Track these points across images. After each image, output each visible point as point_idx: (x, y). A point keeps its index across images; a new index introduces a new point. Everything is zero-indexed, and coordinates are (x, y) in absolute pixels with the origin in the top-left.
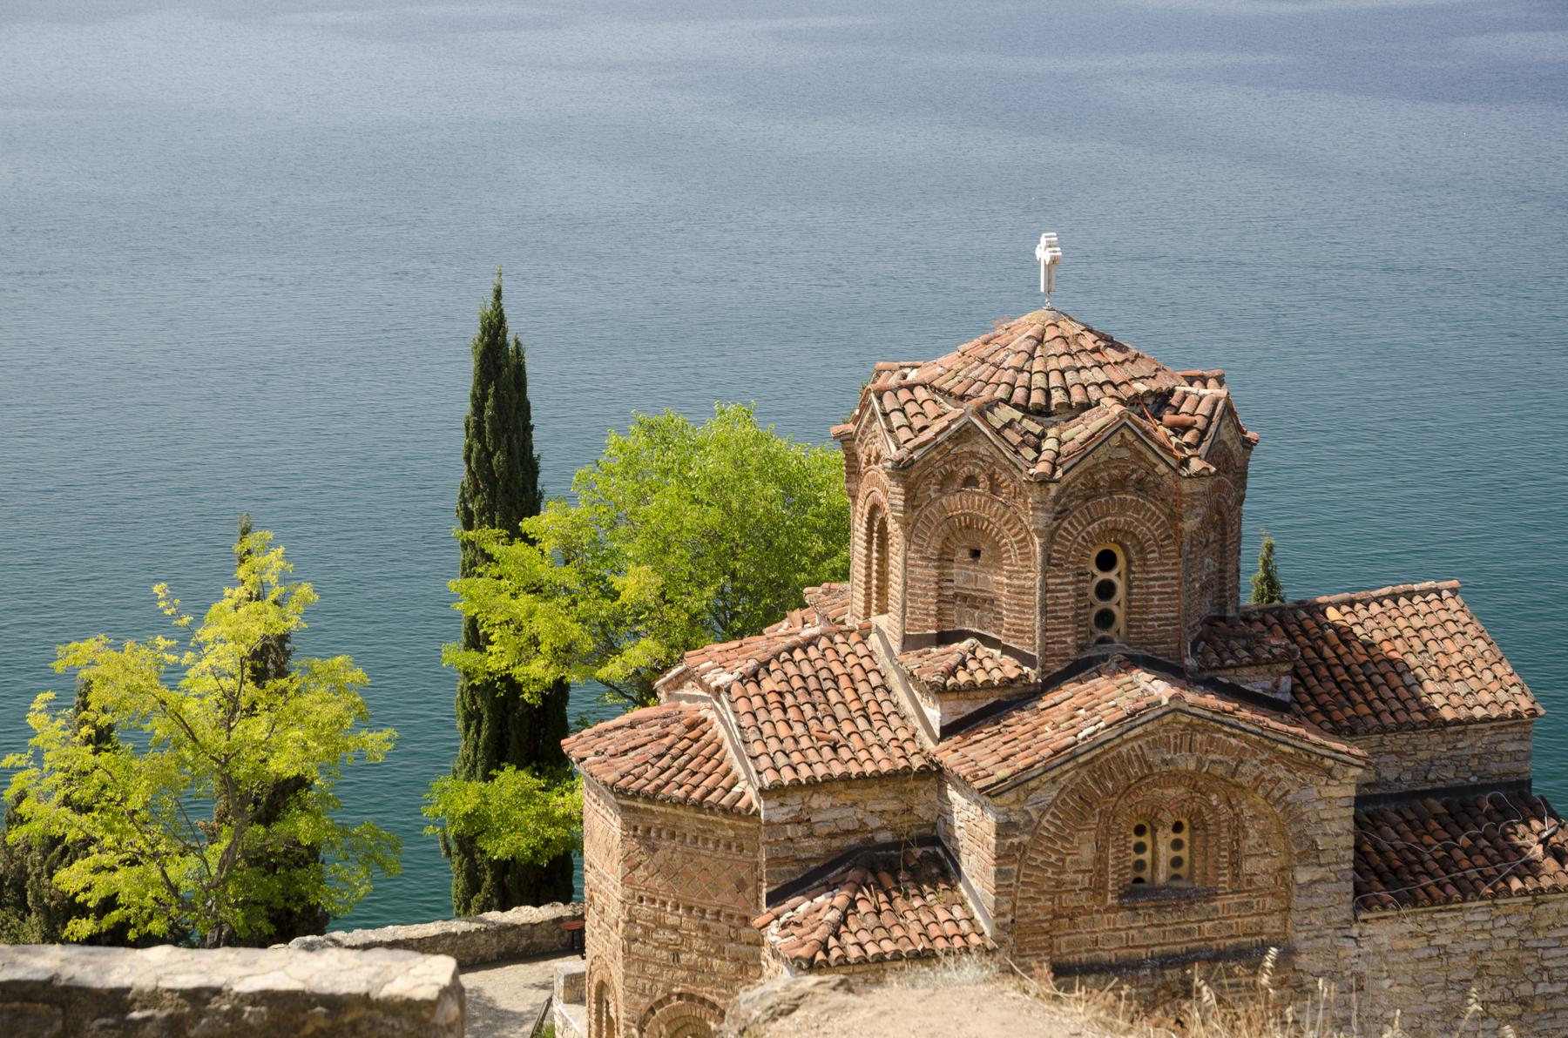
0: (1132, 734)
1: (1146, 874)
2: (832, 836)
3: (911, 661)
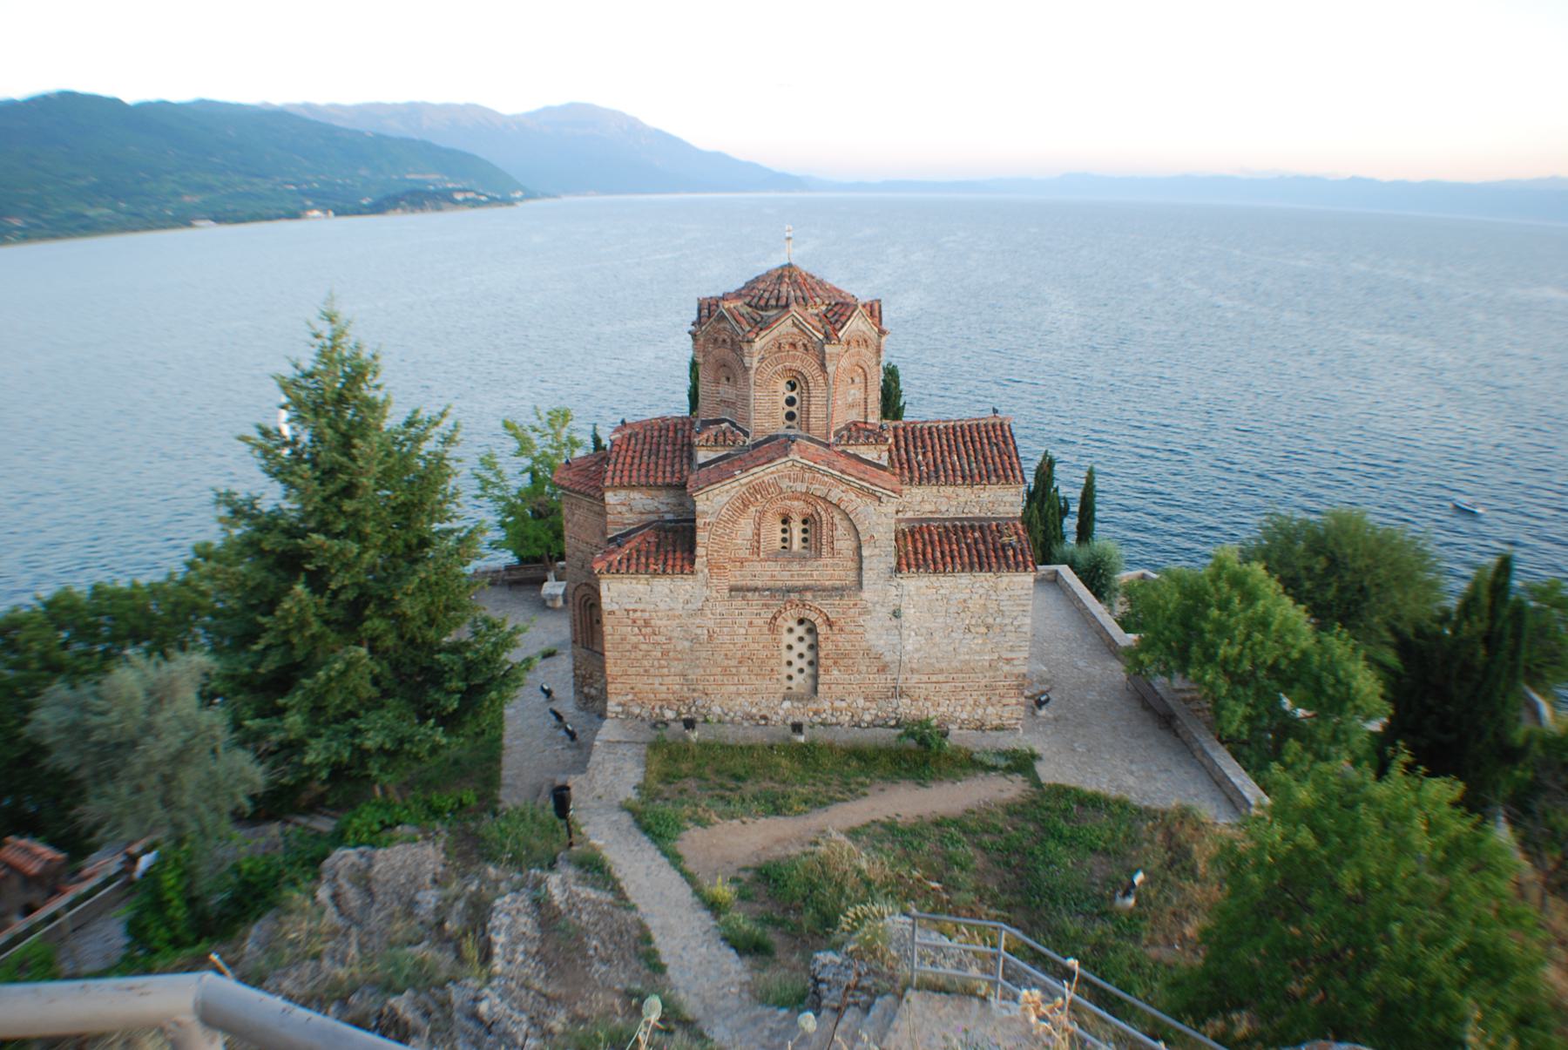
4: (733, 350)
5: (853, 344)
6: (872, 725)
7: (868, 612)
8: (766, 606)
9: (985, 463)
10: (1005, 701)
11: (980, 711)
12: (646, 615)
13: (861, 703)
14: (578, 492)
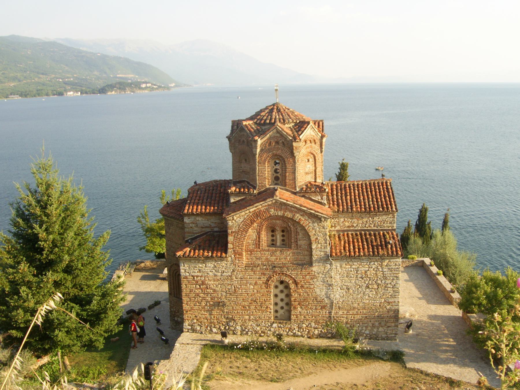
0: (264, 205)
1: (274, 243)
2: (202, 228)
4: (248, 145)
5: (308, 142)
8: (264, 274)
9: (377, 202)
10: (388, 324)
11: (375, 330)
13: (313, 325)
14: (171, 217)
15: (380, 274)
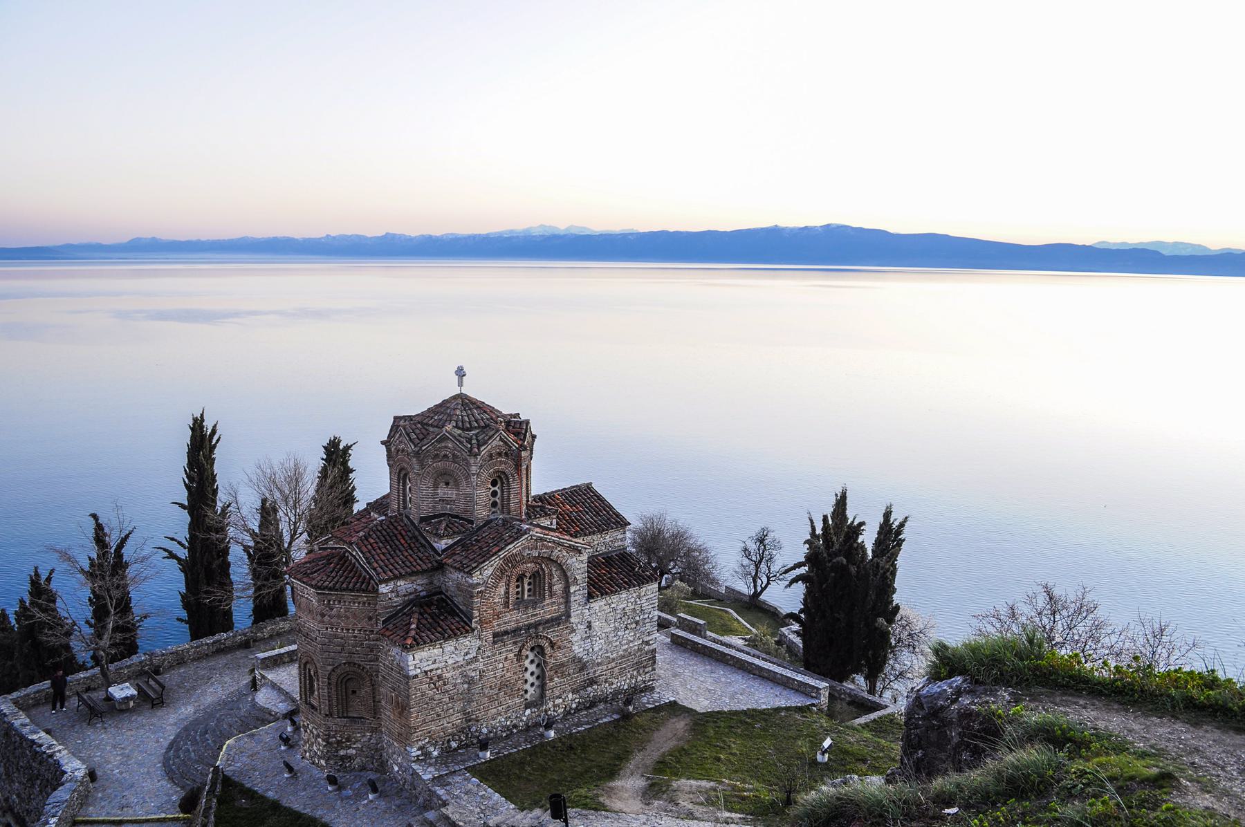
3: (423, 525)
6: (577, 710)
7: (573, 631)
8: (515, 643)
12: (439, 672)
13: (570, 696)
15: (638, 608)
